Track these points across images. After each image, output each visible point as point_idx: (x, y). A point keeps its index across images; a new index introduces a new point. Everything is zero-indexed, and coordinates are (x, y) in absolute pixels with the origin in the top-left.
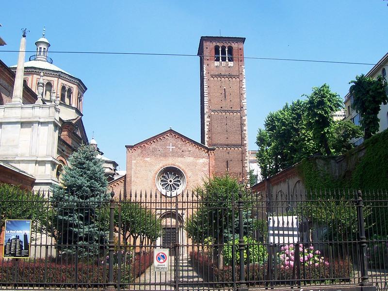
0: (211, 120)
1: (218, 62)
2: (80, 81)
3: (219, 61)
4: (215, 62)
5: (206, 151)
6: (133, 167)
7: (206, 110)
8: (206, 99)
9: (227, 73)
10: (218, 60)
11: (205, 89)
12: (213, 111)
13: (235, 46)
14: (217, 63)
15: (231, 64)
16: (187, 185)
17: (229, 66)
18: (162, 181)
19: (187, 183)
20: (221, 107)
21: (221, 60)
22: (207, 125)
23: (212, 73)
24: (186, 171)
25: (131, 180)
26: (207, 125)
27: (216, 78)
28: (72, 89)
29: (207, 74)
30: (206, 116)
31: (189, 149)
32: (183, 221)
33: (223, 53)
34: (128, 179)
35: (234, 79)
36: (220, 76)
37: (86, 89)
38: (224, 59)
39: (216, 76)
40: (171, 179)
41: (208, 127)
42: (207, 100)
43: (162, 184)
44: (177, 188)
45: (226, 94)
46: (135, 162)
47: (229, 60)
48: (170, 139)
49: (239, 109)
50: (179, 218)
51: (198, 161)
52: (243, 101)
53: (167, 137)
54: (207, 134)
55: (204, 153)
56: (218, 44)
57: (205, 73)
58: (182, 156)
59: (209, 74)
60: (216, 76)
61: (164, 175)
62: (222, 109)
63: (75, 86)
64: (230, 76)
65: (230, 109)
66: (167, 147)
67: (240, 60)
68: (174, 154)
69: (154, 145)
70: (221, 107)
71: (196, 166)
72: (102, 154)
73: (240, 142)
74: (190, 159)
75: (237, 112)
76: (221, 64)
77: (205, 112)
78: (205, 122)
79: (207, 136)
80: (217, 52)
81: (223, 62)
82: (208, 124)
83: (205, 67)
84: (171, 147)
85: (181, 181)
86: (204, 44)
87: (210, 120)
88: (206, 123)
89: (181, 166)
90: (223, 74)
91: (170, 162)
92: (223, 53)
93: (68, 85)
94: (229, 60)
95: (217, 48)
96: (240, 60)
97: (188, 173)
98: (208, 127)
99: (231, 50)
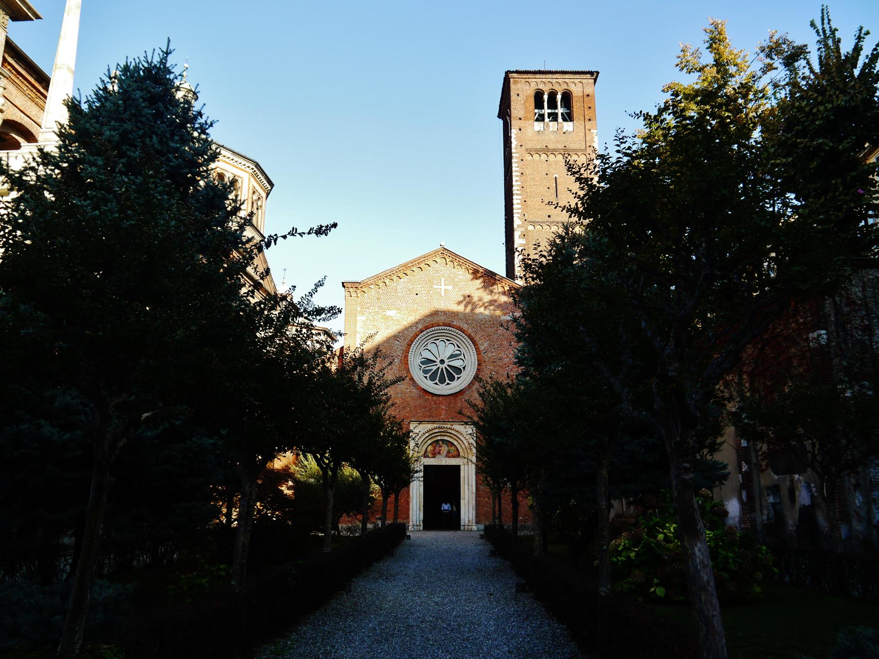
1: (542, 124)
2: (257, 165)
3: (543, 120)
4: (536, 123)
6: (359, 328)
7: (517, 222)
8: (516, 200)
9: (560, 146)
10: (541, 118)
12: (533, 223)
14: (539, 126)
15: (568, 126)
17: (564, 130)
20: (549, 216)
23: (530, 145)
24: (477, 339)
27: (536, 156)
28: (240, 180)
29: (519, 149)
30: (517, 234)
33: (552, 104)
37: (272, 185)
38: (554, 117)
39: (538, 151)
42: (519, 201)
44: (456, 376)
45: (559, 188)
46: (364, 318)
47: (564, 120)
48: (442, 268)
56: (541, 87)
57: (513, 146)
59: (524, 147)
60: (538, 151)
62: (550, 219)
63: (247, 175)
67: (587, 118)
70: (549, 216)
76: (548, 126)
77: (515, 226)
80: (539, 104)
81: (551, 123)
83: (514, 133)
84: (443, 287)
86: (513, 86)
90: (551, 147)
92: (552, 104)
94: (564, 120)
95: (538, 96)
96: (587, 118)
99: (567, 98)
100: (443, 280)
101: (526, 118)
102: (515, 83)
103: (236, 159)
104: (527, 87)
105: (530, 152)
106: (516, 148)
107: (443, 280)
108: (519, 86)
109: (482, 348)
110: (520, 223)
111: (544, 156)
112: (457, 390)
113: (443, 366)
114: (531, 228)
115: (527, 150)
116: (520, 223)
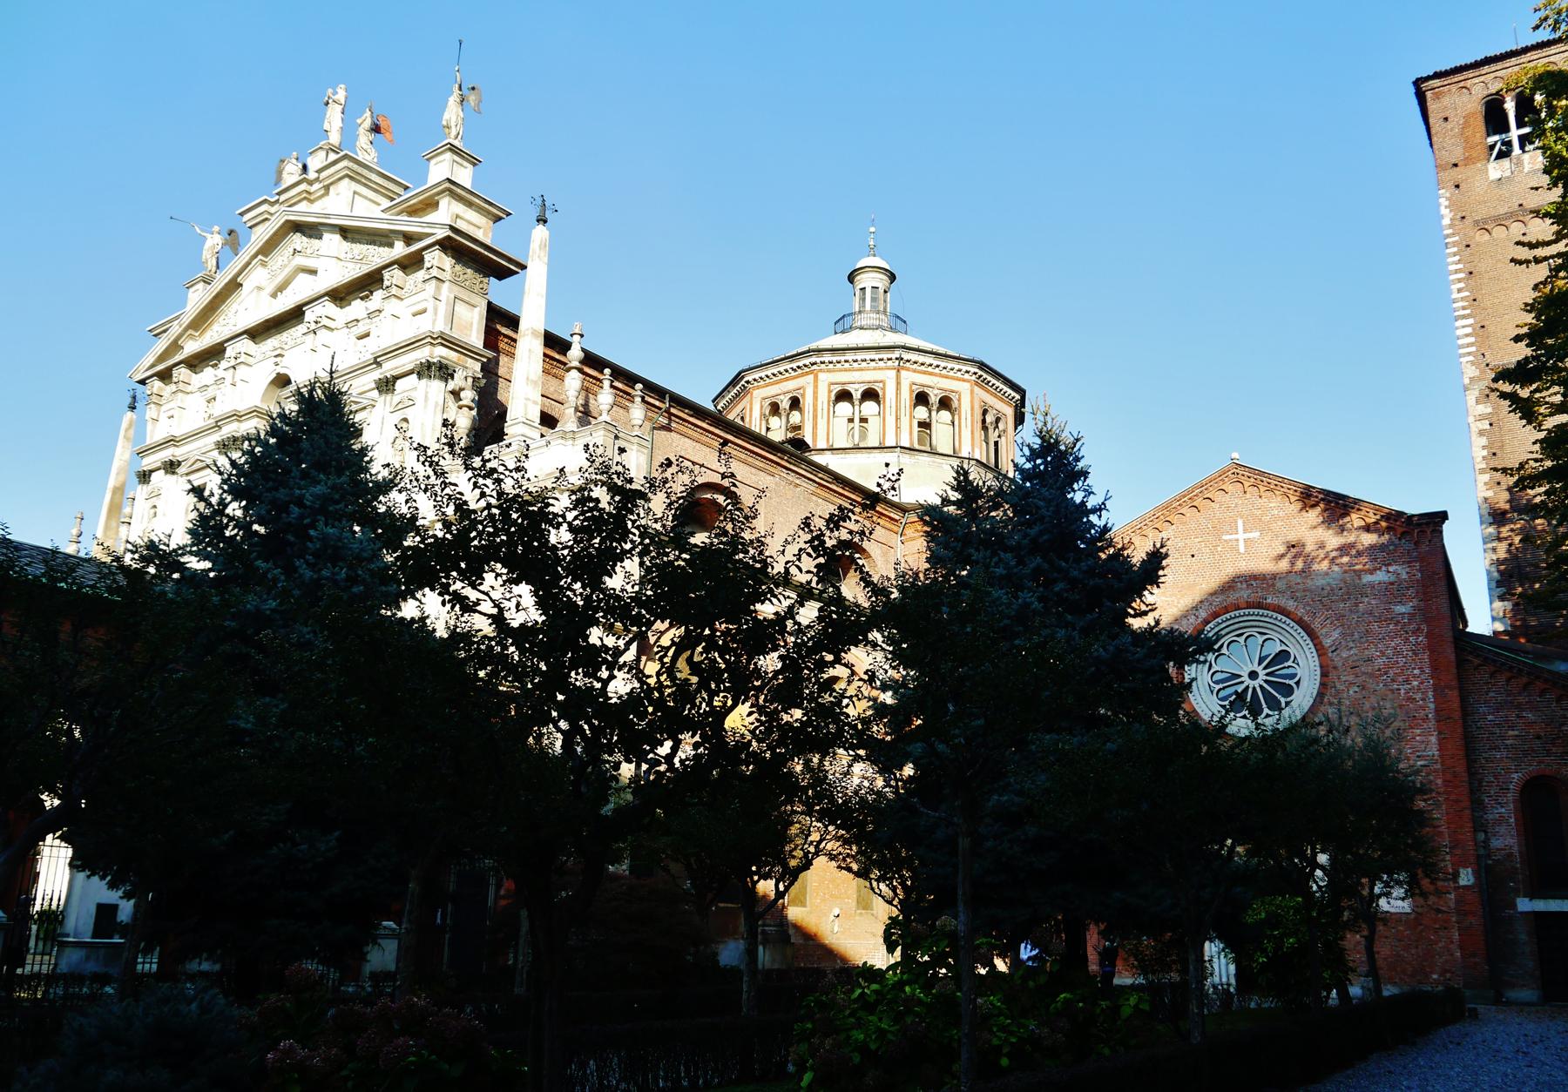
2: (982, 366)
14: (1496, 170)
22: (1481, 433)
23: (1482, 212)
24: (1316, 625)
26: (1481, 433)
41: (1484, 441)
42: (1469, 330)
48: (1234, 498)
53: (1218, 496)
59: (1468, 221)
60: (1500, 221)
63: (967, 385)
76: (1519, 163)
82: (1485, 425)
87: (1489, 410)
93: (937, 385)
98: (1484, 441)
100: (1240, 523)
101: (1468, 161)
102: (1437, 97)
103: (943, 364)
104: (1466, 98)
106: (1451, 226)
107: (1240, 523)
108: (1446, 100)
109: (1327, 642)
110: (1477, 373)
113: (1256, 683)
115: (1477, 222)
116: (1477, 373)
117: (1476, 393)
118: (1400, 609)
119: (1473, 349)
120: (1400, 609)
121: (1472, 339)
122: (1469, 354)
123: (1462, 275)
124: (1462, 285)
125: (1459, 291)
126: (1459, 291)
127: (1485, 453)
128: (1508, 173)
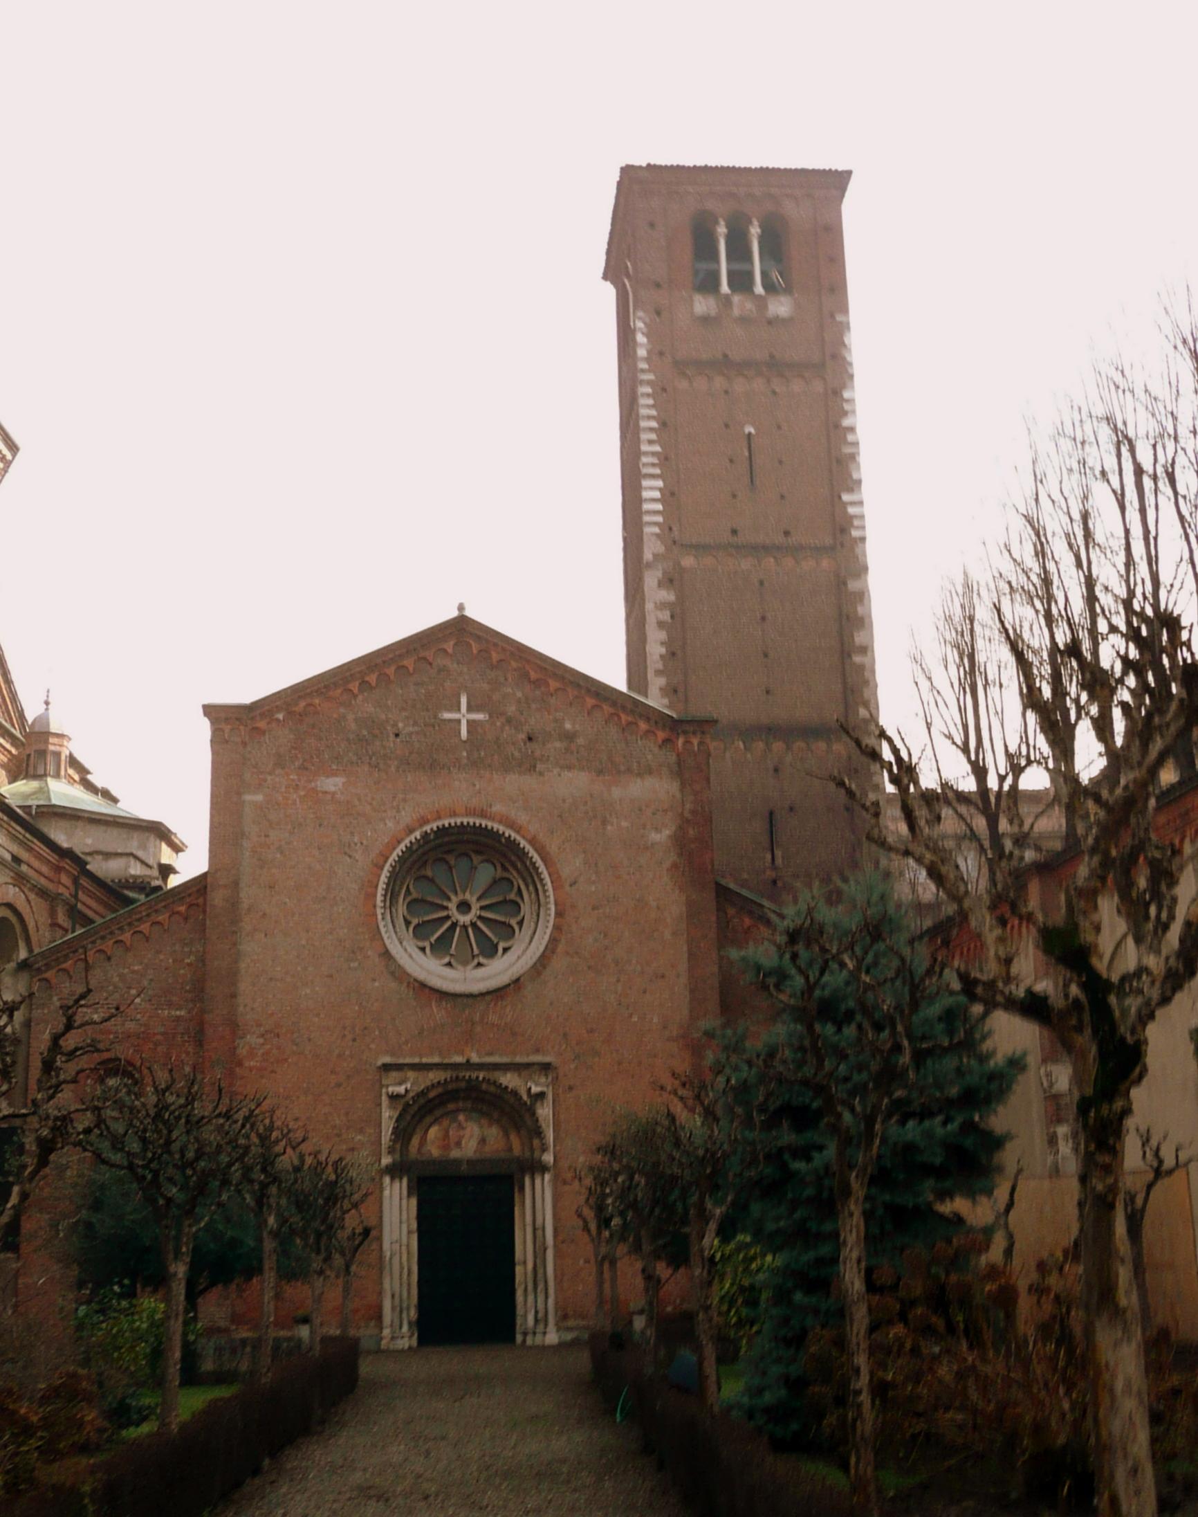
0: (681, 599)
5: (661, 735)
7: (651, 548)
8: (652, 490)
10: (708, 284)
11: (644, 436)
13: (796, 212)
14: (702, 305)
15: (781, 307)
16: (557, 928)
18: (413, 905)
19: (559, 914)
20: (734, 532)
21: (725, 288)
22: (661, 624)
24: (553, 848)
25: (234, 903)
26: (661, 624)
27: (701, 384)
30: (651, 580)
31: (568, 726)
32: (538, 1132)
33: (739, 250)
34: (217, 898)
35: (797, 386)
36: (726, 365)
37: (14, 448)
39: (702, 366)
40: (466, 906)
42: (657, 494)
43: (415, 921)
46: (259, 798)
49: (828, 541)
50: (514, 1113)
51: (616, 792)
52: (846, 497)
53: (441, 661)
54: (658, 673)
55: (649, 750)
56: (711, 205)
57: (642, 353)
58: (529, 766)
60: (702, 366)
61: (429, 873)
64: (775, 367)
65: (779, 539)
66: (447, 715)
68: (483, 753)
69: (366, 706)
71: (604, 822)
72: (115, 800)
73: (832, 713)
74: (572, 784)
75: (819, 550)
76: (727, 301)
78: (649, 606)
79: (662, 681)
81: (736, 299)
82: (665, 616)
85: (526, 908)
88: (653, 615)
89: (522, 818)
91: (456, 799)
92: (739, 250)
97: (564, 864)
98: (663, 635)
100: (464, 700)
105: (681, 367)
107: (464, 700)
109: (566, 872)
110: (660, 548)
111: (719, 382)
112: (504, 979)
114: (688, 561)
117: (659, 574)
118: (655, 837)
119: (660, 519)
120: (655, 837)
121: (659, 507)
122: (656, 524)
123: (654, 424)
124: (653, 436)
125: (651, 442)
126: (651, 442)
127: (663, 650)
128: (713, 313)
